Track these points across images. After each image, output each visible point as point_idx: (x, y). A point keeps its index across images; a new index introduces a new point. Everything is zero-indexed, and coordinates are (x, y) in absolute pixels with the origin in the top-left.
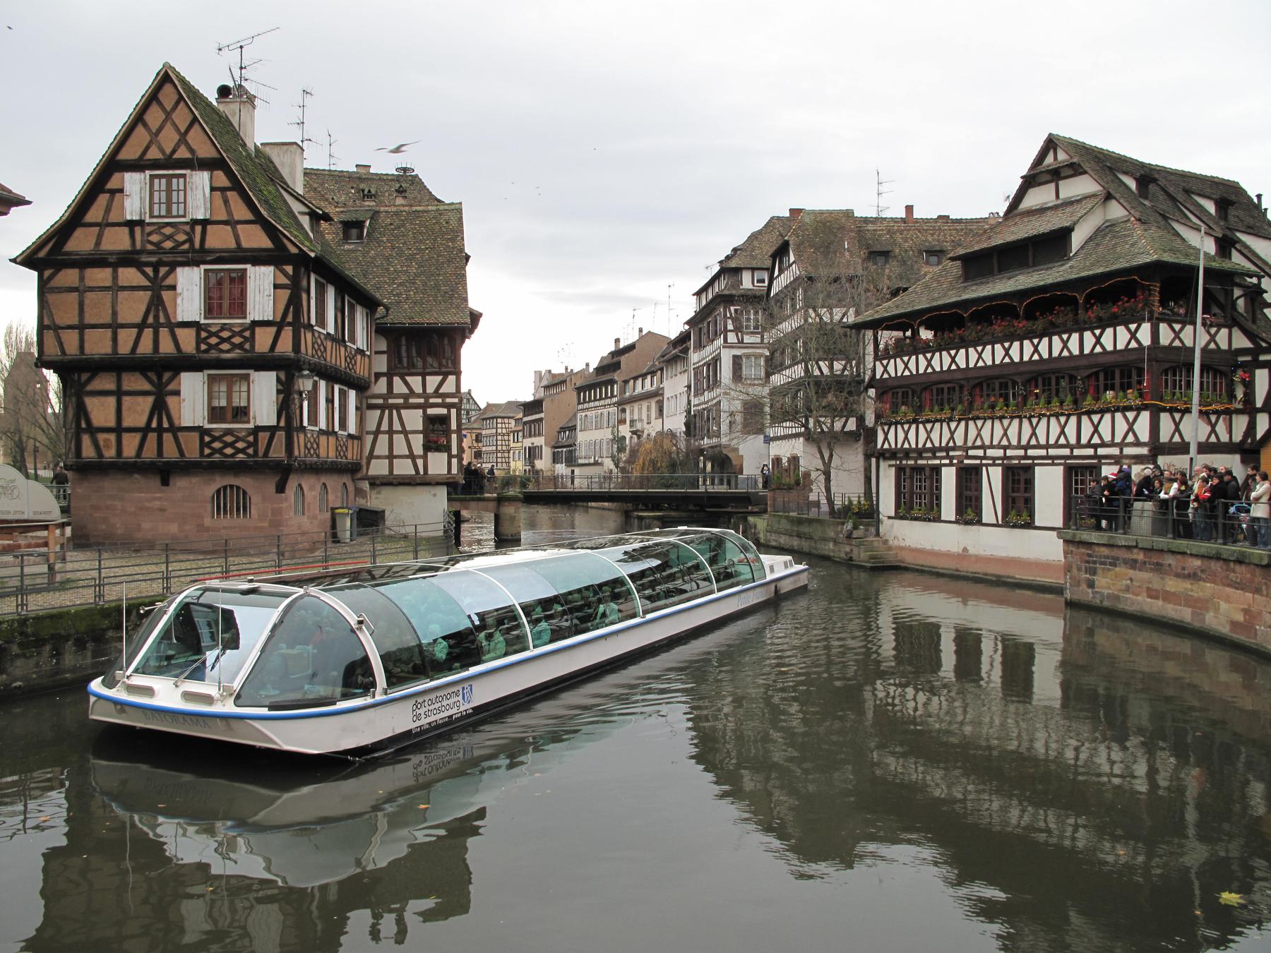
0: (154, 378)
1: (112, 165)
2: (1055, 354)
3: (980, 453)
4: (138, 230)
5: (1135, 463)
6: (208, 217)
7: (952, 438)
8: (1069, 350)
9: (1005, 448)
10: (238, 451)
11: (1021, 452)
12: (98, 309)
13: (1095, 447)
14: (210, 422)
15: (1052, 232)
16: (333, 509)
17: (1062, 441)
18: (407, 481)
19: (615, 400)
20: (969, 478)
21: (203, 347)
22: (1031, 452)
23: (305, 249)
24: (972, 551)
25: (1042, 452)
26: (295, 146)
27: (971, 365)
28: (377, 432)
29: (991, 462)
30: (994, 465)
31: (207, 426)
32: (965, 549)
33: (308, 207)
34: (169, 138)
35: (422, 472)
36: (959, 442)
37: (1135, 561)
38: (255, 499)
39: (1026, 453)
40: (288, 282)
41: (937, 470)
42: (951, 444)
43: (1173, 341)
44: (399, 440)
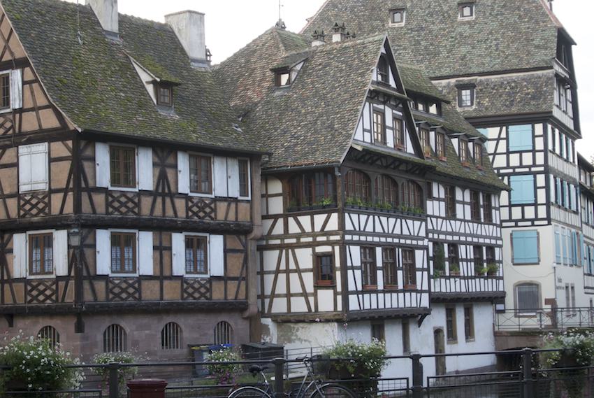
6: (21, 106)
10: (48, 297)
14: (31, 273)
16: (190, 346)
18: (302, 318)
21: (22, 213)
28: (277, 272)
35: (313, 310)
40: (70, 154)
44: (294, 277)
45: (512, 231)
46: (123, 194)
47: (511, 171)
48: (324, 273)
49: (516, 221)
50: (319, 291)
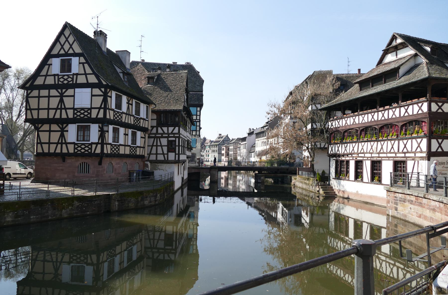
0: (61, 126)
1: (49, 56)
2: (390, 117)
3: (363, 155)
4: (56, 77)
5: (421, 160)
7: (353, 149)
8: (395, 115)
9: (371, 153)
11: (377, 155)
12: (44, 103)
13: (405, 153)
14: (77, 141)
15: (392, 70)
17: (392, 151)
19: (266, 137)
20: (359, 164)
22: (381, 155)
23: (108, 82)
24: (360, 192)
25: (385, 155)
26: (126, 52)
27: (360, 122)
28: (153, 146)
29: (366, 159)
30: (368, 160)
31: (76, 142)
32: (357, 192)
33: (122, 70)
34: (67, 47)
35: (166, 159)
36: (356, 151)
37: (412, 201)
38: (91, 167)
39: (379, 155)
41: (348, 162)
42: (353, 152)
43: (438, 110)
44: (159, 148)
46: (118, 112)
48: (171, 147)
50: (169, 153)
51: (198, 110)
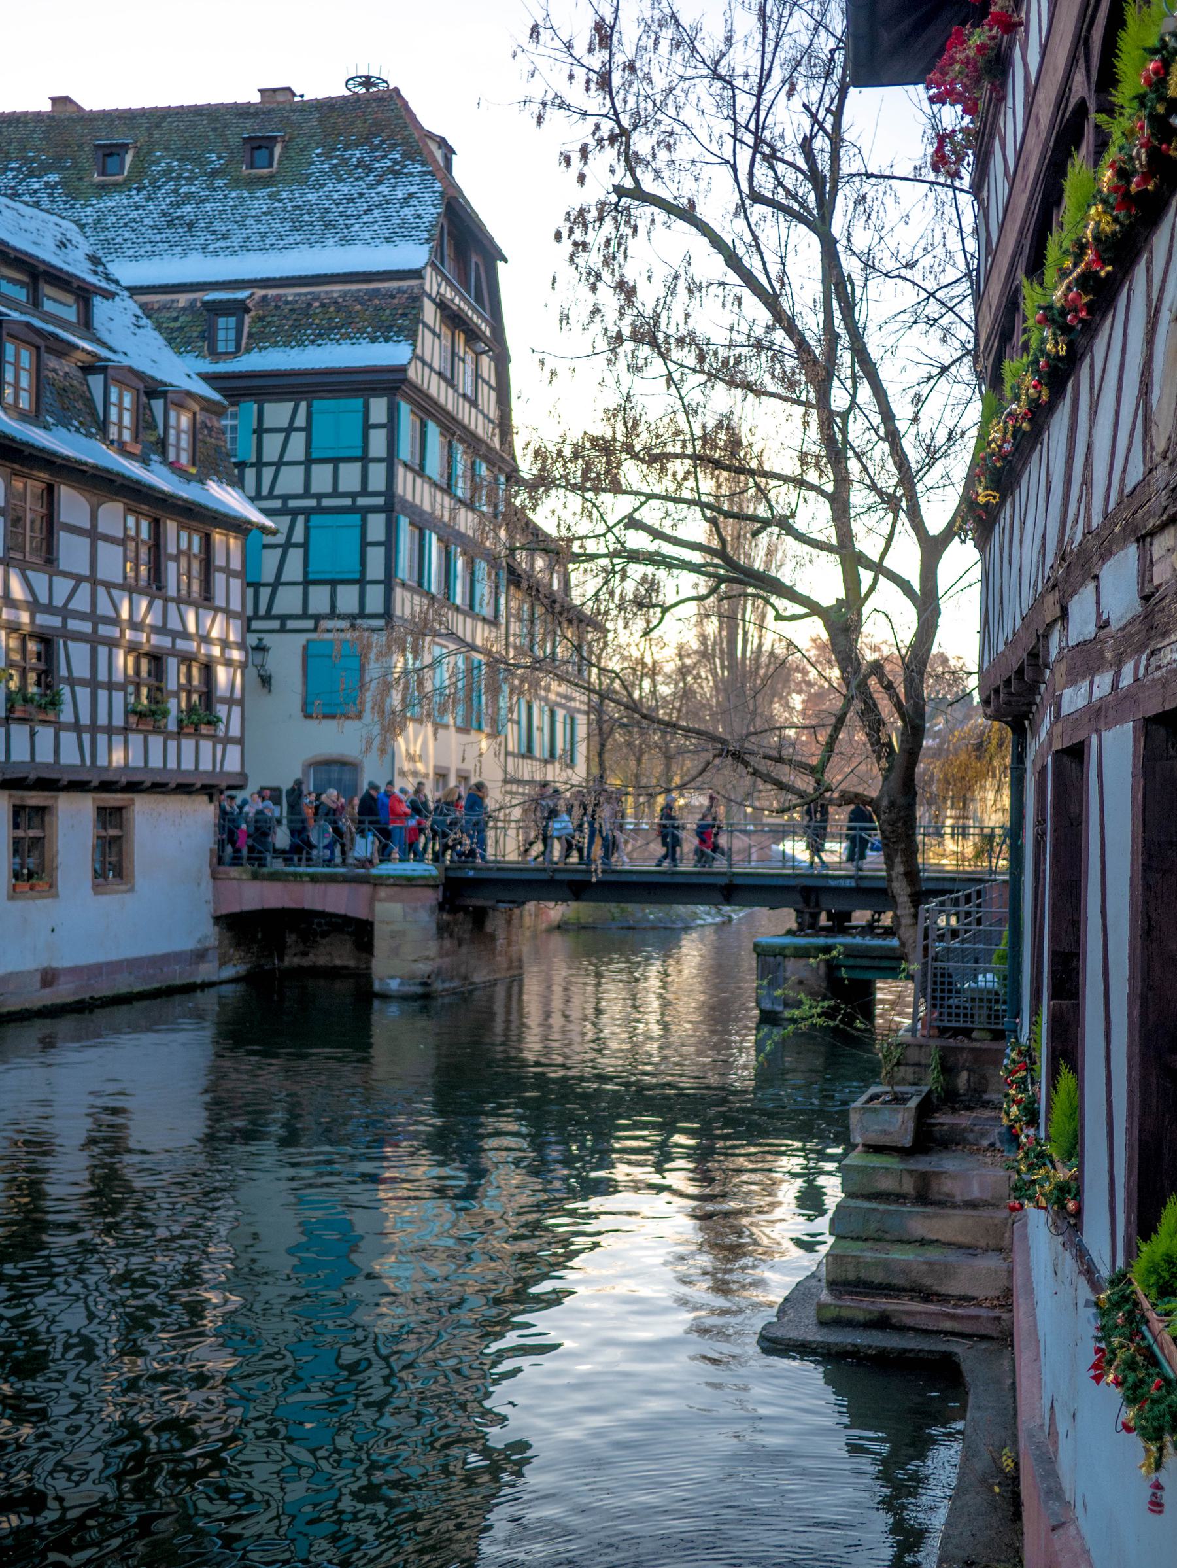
45: (308, 641)
47: (312, 503)
49: (317, 618)
51: (373, 420)
